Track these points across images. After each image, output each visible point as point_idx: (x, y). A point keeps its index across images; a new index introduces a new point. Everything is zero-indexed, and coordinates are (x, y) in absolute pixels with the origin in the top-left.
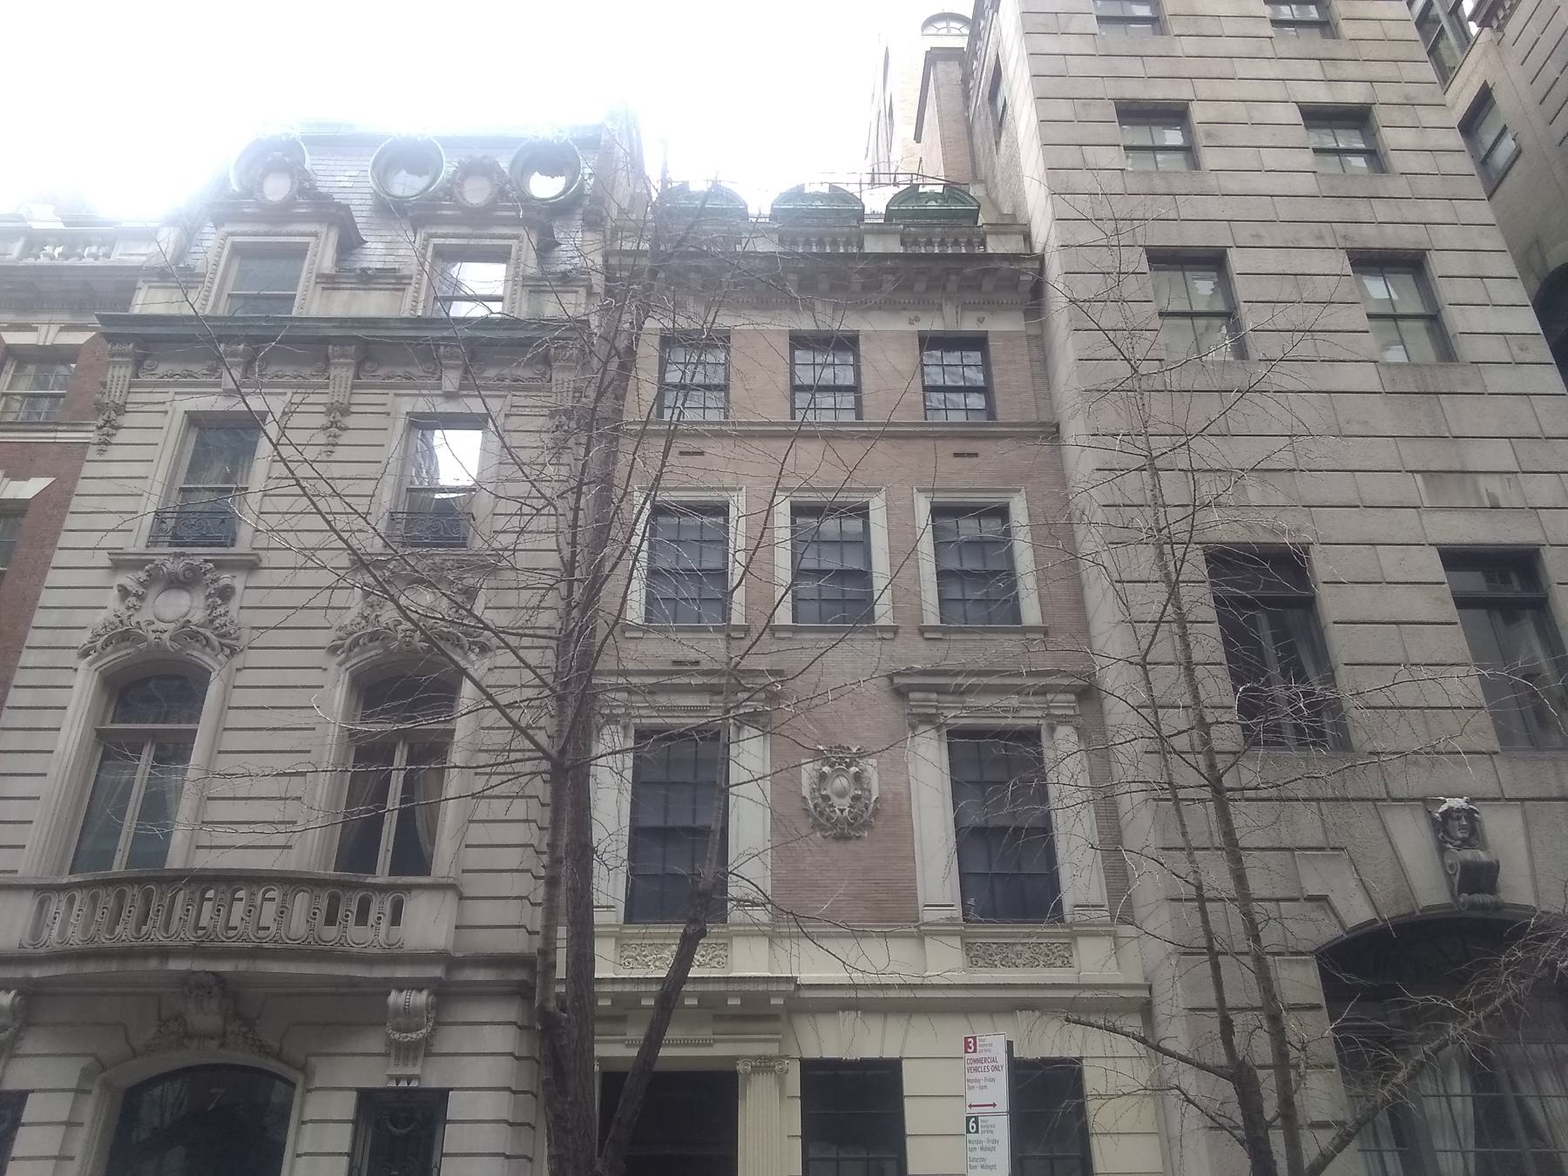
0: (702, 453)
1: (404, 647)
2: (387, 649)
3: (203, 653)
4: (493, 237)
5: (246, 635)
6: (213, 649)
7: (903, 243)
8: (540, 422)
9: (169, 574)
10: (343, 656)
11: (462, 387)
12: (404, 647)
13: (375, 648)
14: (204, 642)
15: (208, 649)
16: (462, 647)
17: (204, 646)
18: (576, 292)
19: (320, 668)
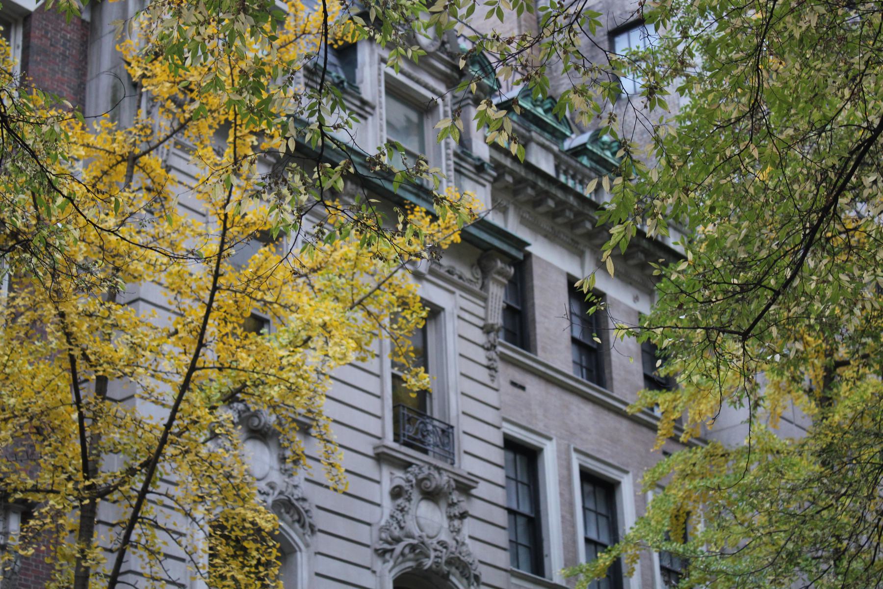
0: (523, 388)
1: (434, 566)
2: (420, 564)
3: (291, 526)
4: (426, 86)
5: (315, 512)
6: (303, 526)
7: (557, 168)
8: (479, 336)
9: (265, 424)
10: (391, 564)
11: (431, 272)
12: (434, 566)
13: (410, 560)
14: (296, 517)
15: (297, 525)
16: (468, 579)
17: (294, 521)
18: (484, 186)
19: (368, 568)
